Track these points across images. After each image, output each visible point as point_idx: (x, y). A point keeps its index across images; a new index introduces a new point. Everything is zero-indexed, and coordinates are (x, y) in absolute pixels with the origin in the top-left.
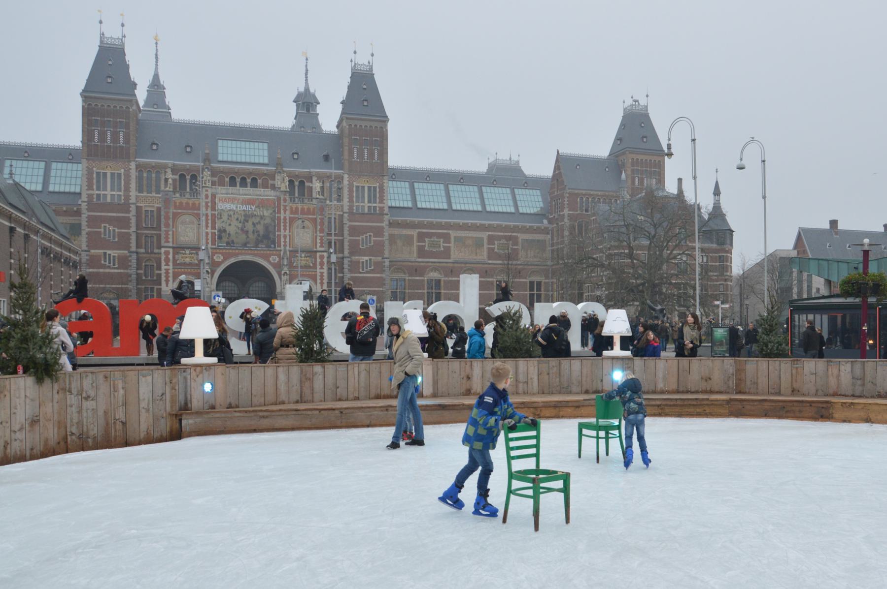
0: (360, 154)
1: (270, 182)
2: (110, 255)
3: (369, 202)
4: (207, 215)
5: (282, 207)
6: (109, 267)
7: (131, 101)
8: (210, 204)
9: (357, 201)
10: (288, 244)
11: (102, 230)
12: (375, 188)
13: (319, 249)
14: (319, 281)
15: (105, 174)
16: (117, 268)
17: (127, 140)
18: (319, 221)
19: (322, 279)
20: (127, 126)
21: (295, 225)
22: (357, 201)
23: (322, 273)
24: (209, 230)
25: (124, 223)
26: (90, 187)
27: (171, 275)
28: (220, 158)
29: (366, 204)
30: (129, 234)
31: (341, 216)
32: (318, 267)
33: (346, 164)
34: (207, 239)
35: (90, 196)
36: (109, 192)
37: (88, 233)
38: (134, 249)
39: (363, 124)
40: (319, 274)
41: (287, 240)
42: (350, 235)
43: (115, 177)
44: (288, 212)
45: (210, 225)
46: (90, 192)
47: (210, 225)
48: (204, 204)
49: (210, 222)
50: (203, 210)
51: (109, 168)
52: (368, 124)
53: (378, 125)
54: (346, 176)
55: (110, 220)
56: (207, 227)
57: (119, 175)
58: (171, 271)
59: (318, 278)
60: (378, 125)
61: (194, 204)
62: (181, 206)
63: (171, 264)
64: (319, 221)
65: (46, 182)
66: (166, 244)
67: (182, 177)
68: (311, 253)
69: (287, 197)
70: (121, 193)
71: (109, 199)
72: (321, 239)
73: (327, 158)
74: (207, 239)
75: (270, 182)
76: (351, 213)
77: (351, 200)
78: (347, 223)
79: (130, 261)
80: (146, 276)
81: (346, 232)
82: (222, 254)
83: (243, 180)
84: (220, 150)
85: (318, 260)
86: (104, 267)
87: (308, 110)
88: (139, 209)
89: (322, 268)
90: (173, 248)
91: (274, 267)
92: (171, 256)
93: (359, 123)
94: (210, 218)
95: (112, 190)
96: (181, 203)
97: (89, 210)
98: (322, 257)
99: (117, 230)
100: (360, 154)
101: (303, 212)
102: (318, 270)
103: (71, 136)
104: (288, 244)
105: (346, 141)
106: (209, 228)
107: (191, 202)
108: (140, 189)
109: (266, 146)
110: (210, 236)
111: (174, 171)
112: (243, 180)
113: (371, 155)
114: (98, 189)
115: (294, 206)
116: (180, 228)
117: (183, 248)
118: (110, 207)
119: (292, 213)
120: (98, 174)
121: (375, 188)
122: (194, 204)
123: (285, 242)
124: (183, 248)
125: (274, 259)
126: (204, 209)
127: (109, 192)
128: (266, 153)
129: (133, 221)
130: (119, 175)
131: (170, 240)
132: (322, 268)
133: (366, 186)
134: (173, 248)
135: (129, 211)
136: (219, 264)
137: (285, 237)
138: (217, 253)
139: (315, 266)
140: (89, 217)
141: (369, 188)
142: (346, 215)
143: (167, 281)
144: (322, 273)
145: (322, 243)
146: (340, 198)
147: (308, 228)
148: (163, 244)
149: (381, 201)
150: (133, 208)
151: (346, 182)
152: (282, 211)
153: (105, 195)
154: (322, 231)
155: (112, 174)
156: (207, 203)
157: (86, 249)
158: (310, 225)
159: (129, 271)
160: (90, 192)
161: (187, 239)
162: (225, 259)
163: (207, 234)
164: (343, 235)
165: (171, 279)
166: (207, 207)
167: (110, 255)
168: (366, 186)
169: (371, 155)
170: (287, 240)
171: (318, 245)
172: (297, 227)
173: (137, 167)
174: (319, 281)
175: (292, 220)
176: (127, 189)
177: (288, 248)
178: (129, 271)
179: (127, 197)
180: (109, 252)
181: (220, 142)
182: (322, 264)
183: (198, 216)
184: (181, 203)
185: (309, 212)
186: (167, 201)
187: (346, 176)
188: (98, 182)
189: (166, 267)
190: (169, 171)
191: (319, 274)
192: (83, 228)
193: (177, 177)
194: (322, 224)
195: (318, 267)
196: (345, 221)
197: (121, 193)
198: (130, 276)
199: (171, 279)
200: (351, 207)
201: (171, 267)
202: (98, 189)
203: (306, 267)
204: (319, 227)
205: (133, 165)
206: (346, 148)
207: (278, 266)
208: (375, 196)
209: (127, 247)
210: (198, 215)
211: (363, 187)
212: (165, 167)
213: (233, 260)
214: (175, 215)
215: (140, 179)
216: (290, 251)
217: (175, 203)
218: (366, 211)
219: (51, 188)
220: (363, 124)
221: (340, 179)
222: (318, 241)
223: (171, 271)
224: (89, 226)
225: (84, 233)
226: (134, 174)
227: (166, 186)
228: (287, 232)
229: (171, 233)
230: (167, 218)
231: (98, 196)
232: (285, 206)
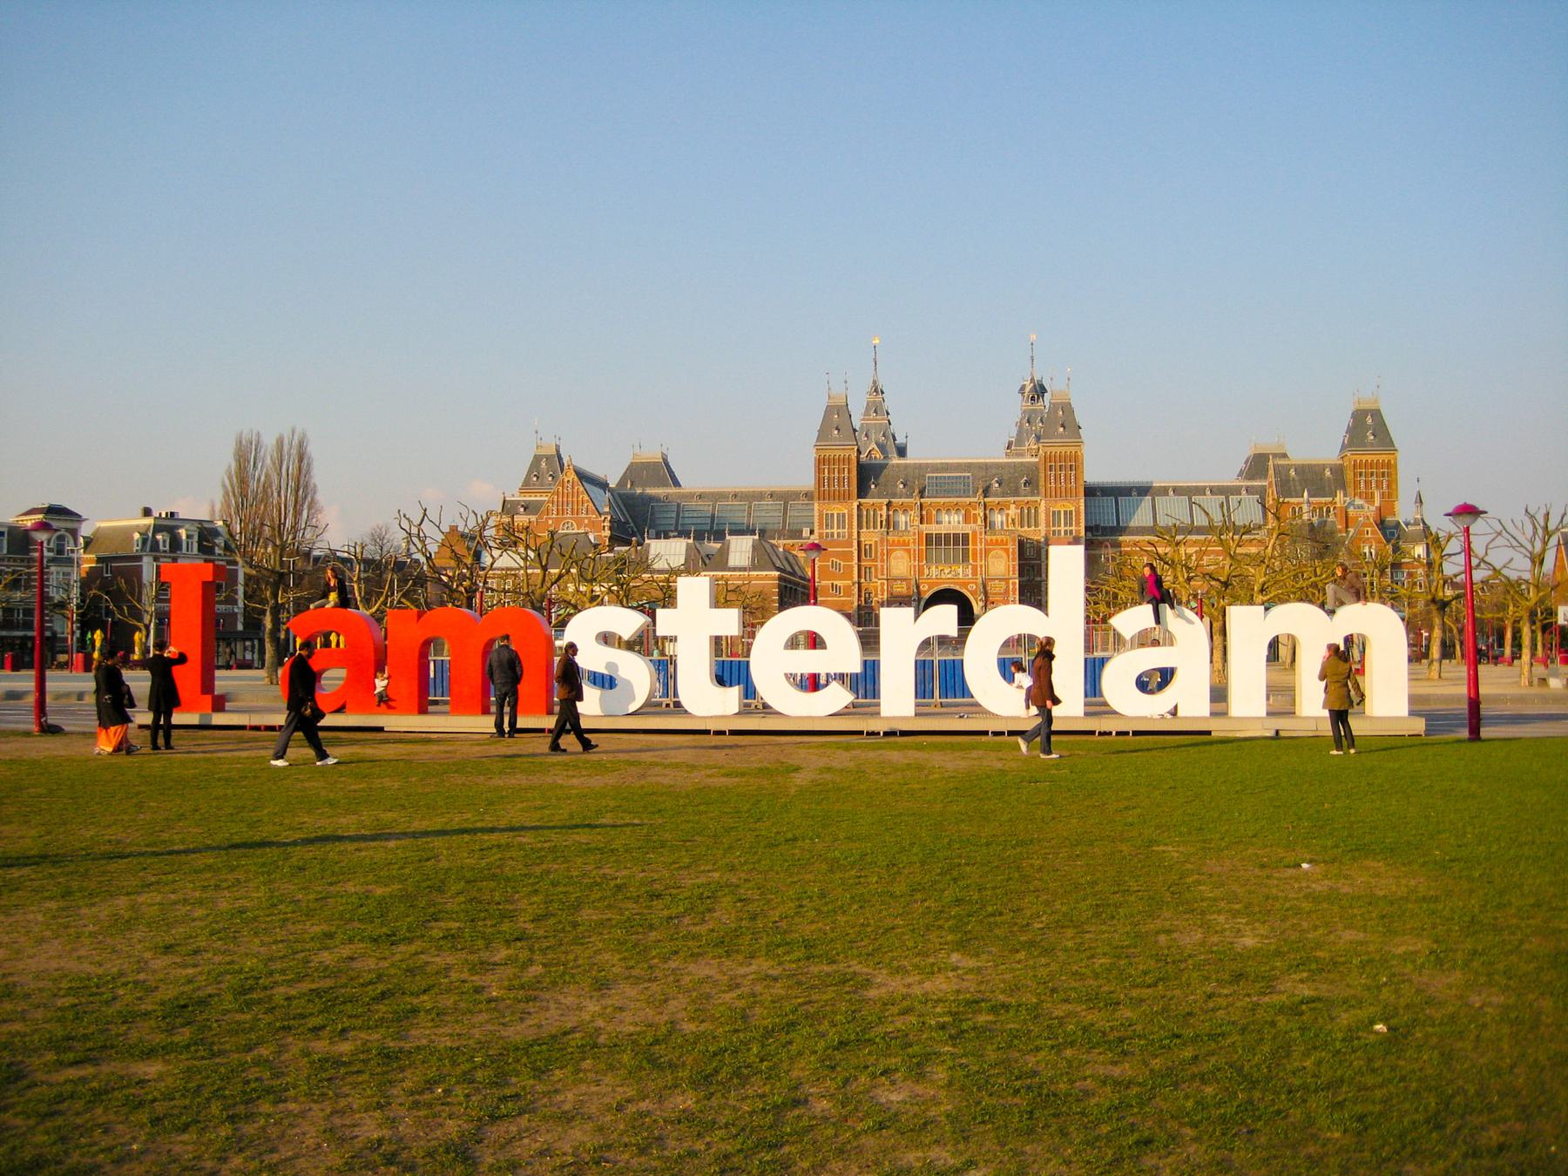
25: (847, 556)
26: (821, 526)
29: (1063, 528)
36: (835, 531)
43: (841, 517)
50: (912, 546)
51: (837, 509)
53: (1073, 450)
60: (1073, 450)
77: (1047, 525)
88: (859, 543)
93: (1054, 450)
103: (805, 480)
108: (860, 526)
116: (893, 562)
127: (835, 531)
149: (1078, 524)
150: (855, 543)
151: (1042, 509)
158: (1003, 553)
175: (987, 552)
179: (850, 535)
183: (908, 551)
185: (1002, 543)
186: (882, 540)
205: (855, 504)
207: (973, 593)
213: (936, 589)
215: (859, 516)
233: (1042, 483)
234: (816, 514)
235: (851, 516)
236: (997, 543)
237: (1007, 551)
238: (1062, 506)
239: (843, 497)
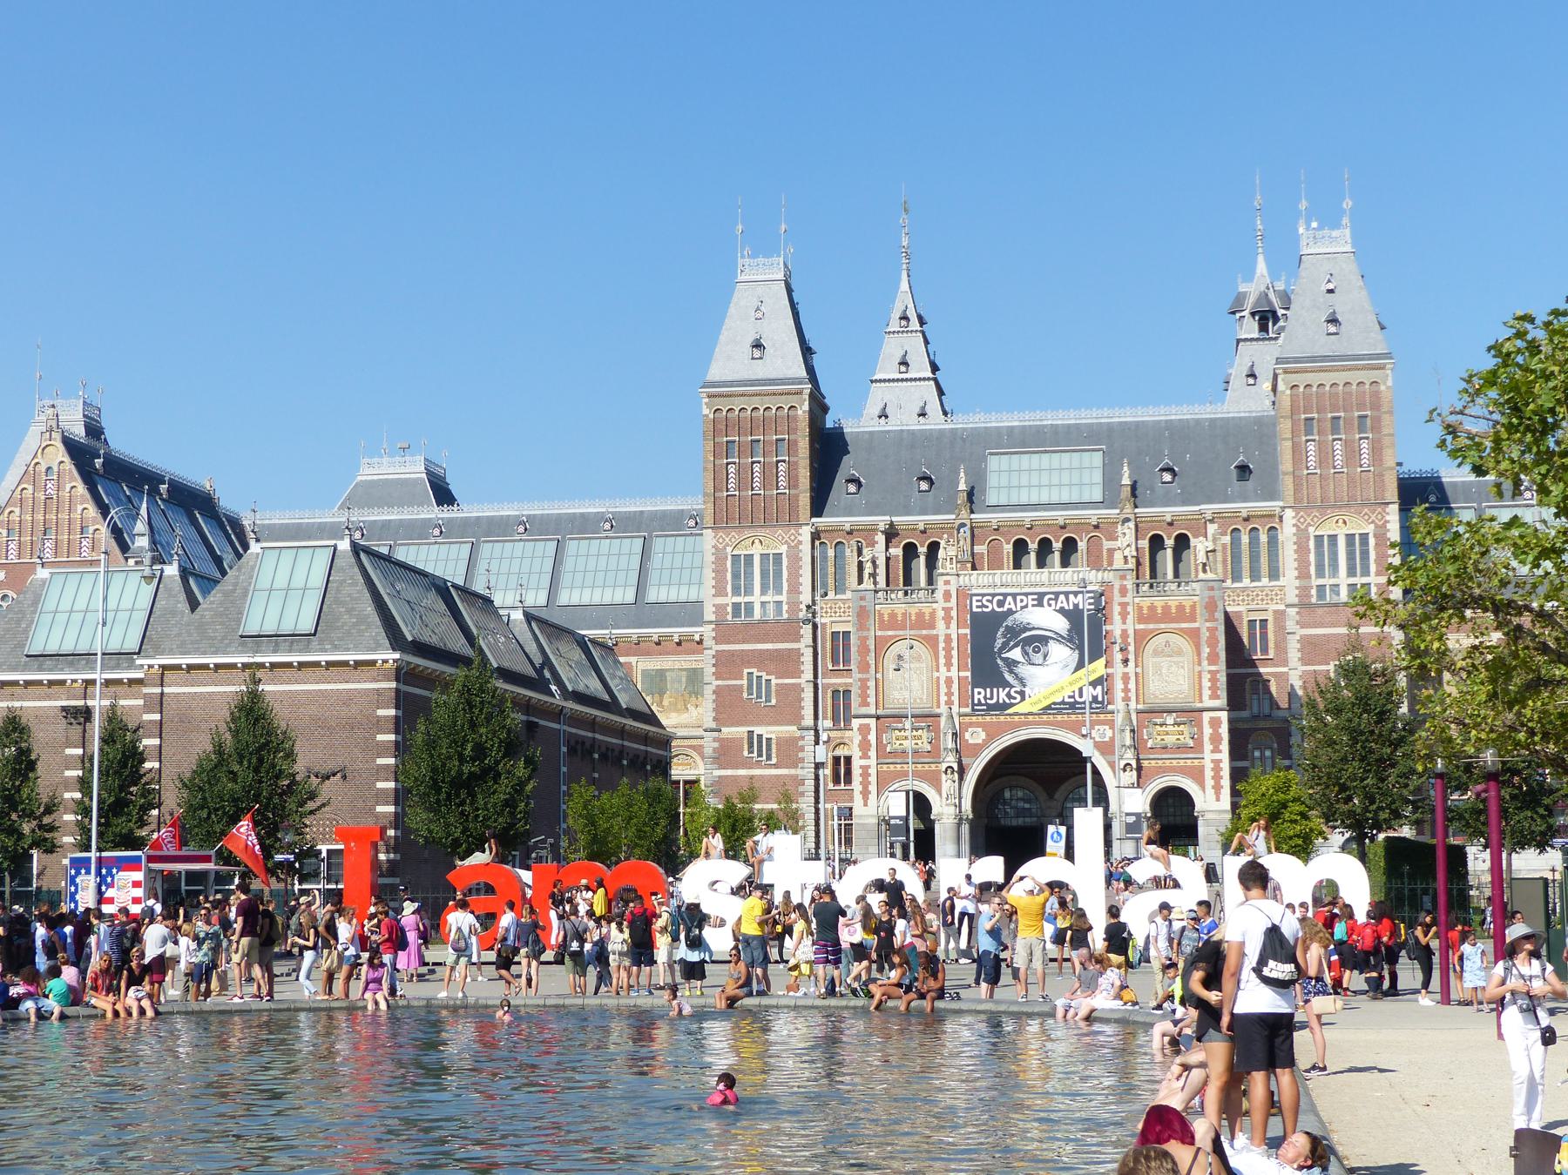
0: (1325, 457)
1: (1107, 545)
2: (760, 736)
3: (1351, 572)
4: (948, 638)
5: (1117, 609)
6: (758, 764)
7: (799, 393)
8: (954, 613)
9: (1320, 574)
10: (1133, 695)
11: (745, 682)
12: (1364, 537)
13: (1208, 703)
14: (1209, 783)
15: (749, 558)
16: (776, 766)
17: (793, 482)
18: (1205, 634)
19: (1217, 778)
20: (792, 447)
21: (1150, 648)
22: (1320, 574)
23: (1217, 762)
24: (954, 673)
25: (787, 664)
26: (720, 591)
27: (873, 779)
28: (992, 499)
29: (1343, 579)
30: (798, 689)
31: (1280, 615)
32: (1208, 747)
33: (1287, 484)
34: (949, 694)
35: (720, 609)
36: (756, 598)
37: (718, 692)
38: (808, 721)
39: (1327, 378)
40: (1208, 766)
41: (1132, 685)
42: (1304, 661)
44: (1130, 618)
45: (955, 661)
46: (720, 600)
47: (955, 661)
48: (941, 614)
49: (955, 653)
50: (941, 625)
52: (1340, 377)
53: (1367, 376)
54: (1289, 514)
55: (760, 659)
56: (949, 665)
57: (778, 557)
58: (873, 771)
59: (1209, 774)
61: (920, 615)
62: (893, 622)
63: (873, 753)
64: (1205, 634)
65: (641, 588)
66: (864, 711)
67: (910, 550)
68: (1190, 714)
69: (1129, 583)
70: (783, 598)
71: (757, 614)
72: (1214, 680)
73: (1244, 470)
74: (949, 694)
75: (1107, 545)
76: (1304, 605)
77: (1303, 574)
78: (1296, 633)
79: (802, 749)
80: (836, 781)
81: (1294, 654)
82: (984, 726)
83: (1020, 547)
84: (992, 480)
85: (1207, 731)
86: (747, 764)
87: (1263, 328)
89: (1216, 750)
90: (878, 718)
91: (1103, 754)
92: (872, 737)
94: (955, 644)
95: (764, 591)
96: (893, 615)
97: (717, 640)
98: (1215, 723)
99: (774, 682)
100: (1325, 457)
101: (1167, 616)
102: (1208, 756)
104: (1133, 695)
105: (1285, 427)
106: (955, 668)
107: (913, 610)
109: (1097, 458)
110: (955, 686)
111: (891, 534)
112: (1045, 546)
113: (1352, 454)
114: (736, 591)
115: (1146, 603)
117: (900, 717)
118: (762, 630)
119: (1141, 619)
120: (736, 558)
121: (1364, 537)
122: (920, 615)
123: (1126, 690)
124: (900, 717)
125: (1103, 733)
126: (941, 625)
127: (756, 598)
128: (1098, 477)
129: (807, 658)
130: (778, 557)
131: (872, 700)
132: (1216, 750)
133: (1341, 532)
134: (878, 718)
135: (797, 638)
136: (977, 750)
137: (1126, 678)
138: (971, 725)
139: (1198, 747)
140: (718, 656)
141: (1350, 537)
142: (1292, 611)
143: (865, 794)
144: (1217, 762)
145: (1214, 688)
146: (1274, 574)
147: (1180, 653)
148: (855, 708)
150: (807, 630)
151: (1287, 532)
152: (1117, 618)
153: (749, 607)
154: (1213, 659)
155: (764, 557)
156: (947, 610)
157: (714, 725)
158: (1185, 644)
159: (799, 772)
160: (720, 600)
161: (906, 694)
162: (991, 737)
163: (949, 681)
164: (1285, 663)
165: (873, 788)
166: (948, 619)
167: (760, 736)
168: (1341, 532)
169: (1352, 454)
170: (1132, 685)
171: (1206, 693)
172: (1156, 653)
173: (816, 536)
174: (1209, 783)
175: (1142, 638)
176: (795, 589)
177: (1133, 705)
178: (799, 772)
179: (794, 605)
180: (758, 730)
181: (994, 463)
182: (1215, 739)
183: (932, 642)
184: (893, 615)
185: (1182, 614)
186: (862, 614)
187: (1289, 514)
188: (736, 576)
189: (864, 762)
190: (881, 539)
191: (1208, 766)
192: (706, 680)
193: (896, 552)
194: (1212, 643)
195: (1208, 747)
196: (1291, 625)
197: (783, 598)
198: (802, 782)
199: (873, 788)
200: (1304, 591)
201: (873, 762)
202: (736, 591)
203: (1180, 748)
204: (1206, 650)
205: (805, 533)
206: (1286, 447)
207: (1106, 748)
208: (1365, 554)
209: (796, 719)
210: (932, 642)
211: (1333, 539)
212: (871, 530)
213: (1007, 740)
214: (882, 645)
216: (1139, 712)
217: (881, 615)
218: (1344, 595)
219: (653, 595)
220: (1327, 378)
221: (1273, 524)
222: (1206, 684)
223: (873, 771)
224: (718, 676)
225: (708, 691)
226: (806, 548)
227: (860, 581)
228: (1131, 664)
229: (872, 684)
230: (864, 650)
231: (736, 606)
232: (1124, 605)
233: (1286, 464)
234: (710, 558)
235: (795, 559)
236: (1167, 616)
237: (1194, 635)
238: (1341, 527)
239: (776, 515)
